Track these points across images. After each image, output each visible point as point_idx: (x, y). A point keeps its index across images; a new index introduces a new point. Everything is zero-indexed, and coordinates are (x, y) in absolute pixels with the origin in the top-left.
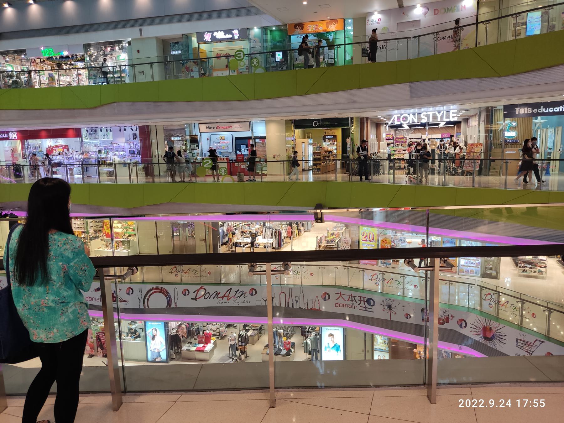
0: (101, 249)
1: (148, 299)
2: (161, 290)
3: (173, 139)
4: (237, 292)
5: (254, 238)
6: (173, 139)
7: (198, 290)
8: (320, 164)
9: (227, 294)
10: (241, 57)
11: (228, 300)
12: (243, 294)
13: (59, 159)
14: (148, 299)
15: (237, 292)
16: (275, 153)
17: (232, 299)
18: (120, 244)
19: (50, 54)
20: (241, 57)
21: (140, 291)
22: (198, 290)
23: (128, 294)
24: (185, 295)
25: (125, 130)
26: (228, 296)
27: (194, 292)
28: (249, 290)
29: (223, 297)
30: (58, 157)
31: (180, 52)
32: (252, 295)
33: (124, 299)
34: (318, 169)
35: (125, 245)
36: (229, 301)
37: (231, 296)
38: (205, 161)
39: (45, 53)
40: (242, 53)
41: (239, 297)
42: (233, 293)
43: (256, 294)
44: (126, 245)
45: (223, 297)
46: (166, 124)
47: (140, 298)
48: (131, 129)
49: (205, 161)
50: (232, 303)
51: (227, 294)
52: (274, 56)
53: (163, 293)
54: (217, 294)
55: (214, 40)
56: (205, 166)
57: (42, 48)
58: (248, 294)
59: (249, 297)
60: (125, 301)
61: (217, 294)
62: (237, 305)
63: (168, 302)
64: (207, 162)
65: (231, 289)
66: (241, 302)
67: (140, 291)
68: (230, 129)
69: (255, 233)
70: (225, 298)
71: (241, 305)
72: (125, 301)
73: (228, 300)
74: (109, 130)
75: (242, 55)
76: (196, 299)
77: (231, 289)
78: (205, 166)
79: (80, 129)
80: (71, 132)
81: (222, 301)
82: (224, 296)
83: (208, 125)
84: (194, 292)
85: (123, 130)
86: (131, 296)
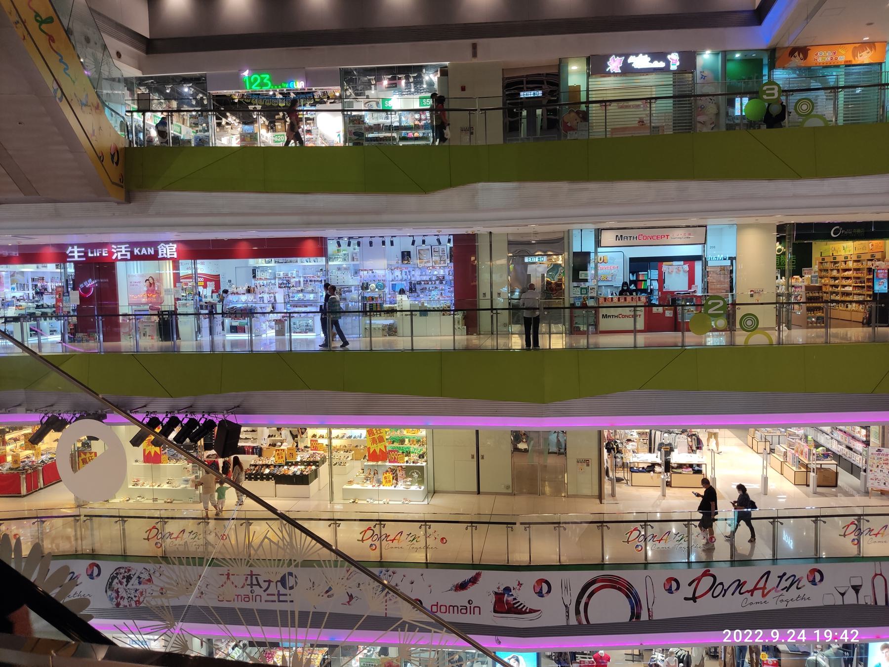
0: (355, 486)
1: (586, 605)
2: (615, 584)
3: (526, 260)
4: (781, 577)
5: (668, 452)
6: (526, 260)
7: (699, 579)
8: (819, 309)
9: (761, 585)
10: (773, 94)
11: (764, 595)
12: (795, 581)
13: (246, 302)
14: (586, 605)
15: (781, 577)
16: (755, 287)
17: (773, 594)
18: (399, 474)
19: (262, 84)
20: (773, 94)
21: (566, 587)
22: (699, 579)
23: (540, 594)
24: (670, 591)
25: (371, 243)
26: (764, 588)
27: (690, 585)
28: (807, 572)
29: (752, 592)
30: (244, 298)
31: (539, 93)
32: (813, 582)
33: (530, 605)
34: (818, 318)
35: (411, 476)
36: (767, 598)
37: (769, 586)
38: (710, 303)
39: (251, 84)
40: (776, 87)
41: (787, 589)
42: (773, 581)
43: (822, 580)
44: (416, 475)
45: (752, 592)
46: (522, 230)
47: (567, 603)
48: (439, 240)
49: (710, 303)
50: (772, 603)
51: (761, 585)
52: (732, 104)
53: (620, 589)
54: (740, 584)
55: (627, 70)
56: (710, 311)
57: (246, 73)
58: (804, 582)
59: (807, 588)
60: (532, 611)
61: (740, 584)
62: (782, 606)
63: (632, 609)
64: (714, 304)
65: (768, 573)
66: (792, 600)
67: (566, 587)
68: (664, 241)
69: (670, 444)
70: (758, 593)
71: (792, 605)
72: (532, 611)
73: (764, 595)
74: (388, 243)
75: (776, 92)
76: (694, 599)
77: (768, 573)
78: (710, 311)
79: (325, 239)
80: (310, 246)
81: (751, 599)
82: (755, 588)
83: (619, 233)
84: (690, 585)
85: (388, 243)
86: (547, 598)
